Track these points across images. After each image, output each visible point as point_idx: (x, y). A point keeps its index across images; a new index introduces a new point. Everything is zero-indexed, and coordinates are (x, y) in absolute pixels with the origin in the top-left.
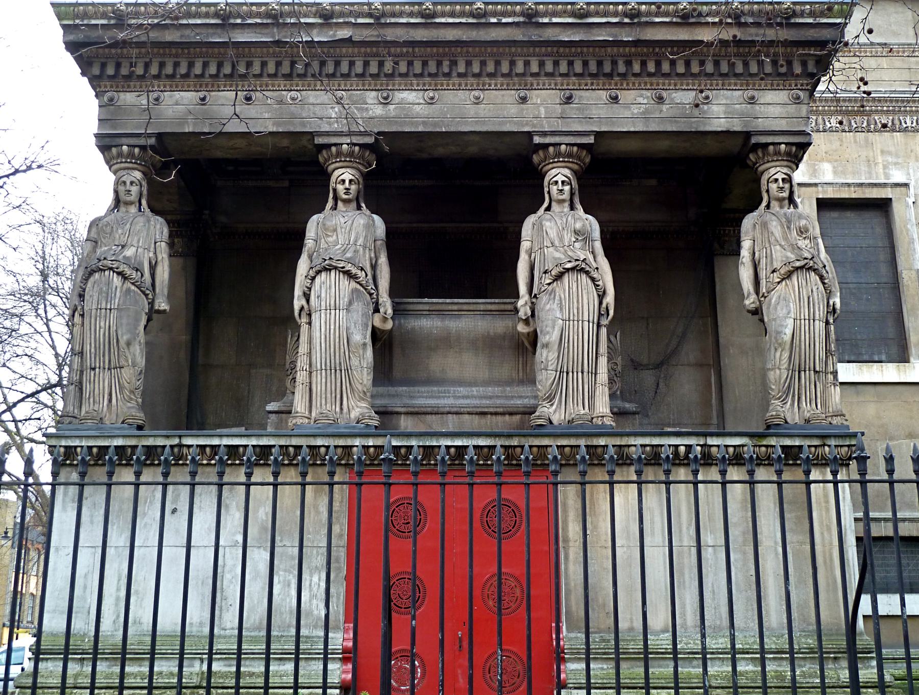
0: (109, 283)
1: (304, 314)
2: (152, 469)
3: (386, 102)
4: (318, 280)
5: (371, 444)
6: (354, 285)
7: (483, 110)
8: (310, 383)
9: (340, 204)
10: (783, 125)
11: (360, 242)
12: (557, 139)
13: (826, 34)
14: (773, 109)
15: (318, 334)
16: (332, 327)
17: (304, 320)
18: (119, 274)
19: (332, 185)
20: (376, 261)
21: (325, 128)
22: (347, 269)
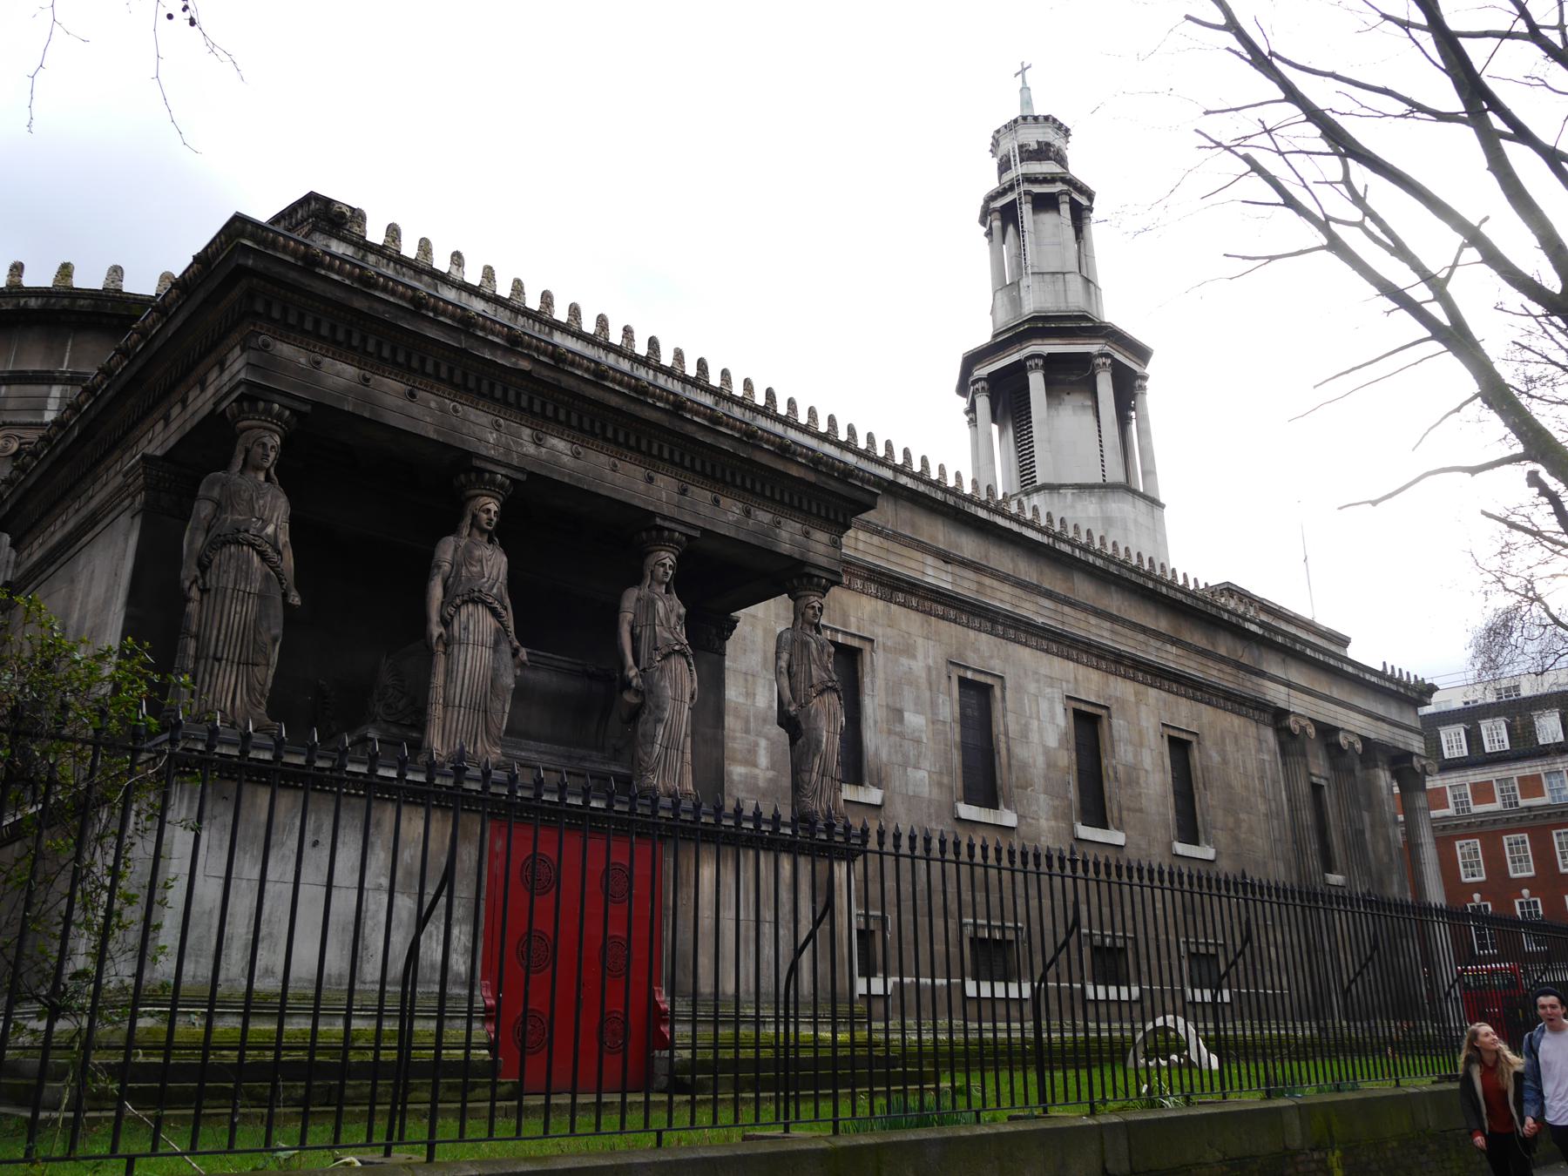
0: (249, 562)
2: (292, 792)
3: (538, 442)
4: (464, 611)
7: (619, 478)
10: (823, 562)
12: (673, 526)
13: (866, 498)
14: (818, 546)
15: (461, 668)
17: (441, 649)
18: (259, 553)
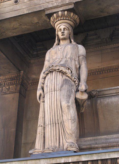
1: (41, 97)
5: (70, 161)
6: (65, 77)
8: (44, 133)
9: (61, 41)
11: (68, 56)
16: (53, 101)
19: (56, 33)
20: (80, 67)
21: (50, 6)
22: (60, 70)
